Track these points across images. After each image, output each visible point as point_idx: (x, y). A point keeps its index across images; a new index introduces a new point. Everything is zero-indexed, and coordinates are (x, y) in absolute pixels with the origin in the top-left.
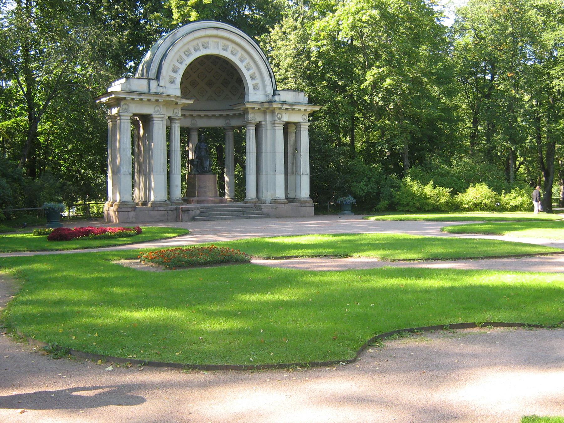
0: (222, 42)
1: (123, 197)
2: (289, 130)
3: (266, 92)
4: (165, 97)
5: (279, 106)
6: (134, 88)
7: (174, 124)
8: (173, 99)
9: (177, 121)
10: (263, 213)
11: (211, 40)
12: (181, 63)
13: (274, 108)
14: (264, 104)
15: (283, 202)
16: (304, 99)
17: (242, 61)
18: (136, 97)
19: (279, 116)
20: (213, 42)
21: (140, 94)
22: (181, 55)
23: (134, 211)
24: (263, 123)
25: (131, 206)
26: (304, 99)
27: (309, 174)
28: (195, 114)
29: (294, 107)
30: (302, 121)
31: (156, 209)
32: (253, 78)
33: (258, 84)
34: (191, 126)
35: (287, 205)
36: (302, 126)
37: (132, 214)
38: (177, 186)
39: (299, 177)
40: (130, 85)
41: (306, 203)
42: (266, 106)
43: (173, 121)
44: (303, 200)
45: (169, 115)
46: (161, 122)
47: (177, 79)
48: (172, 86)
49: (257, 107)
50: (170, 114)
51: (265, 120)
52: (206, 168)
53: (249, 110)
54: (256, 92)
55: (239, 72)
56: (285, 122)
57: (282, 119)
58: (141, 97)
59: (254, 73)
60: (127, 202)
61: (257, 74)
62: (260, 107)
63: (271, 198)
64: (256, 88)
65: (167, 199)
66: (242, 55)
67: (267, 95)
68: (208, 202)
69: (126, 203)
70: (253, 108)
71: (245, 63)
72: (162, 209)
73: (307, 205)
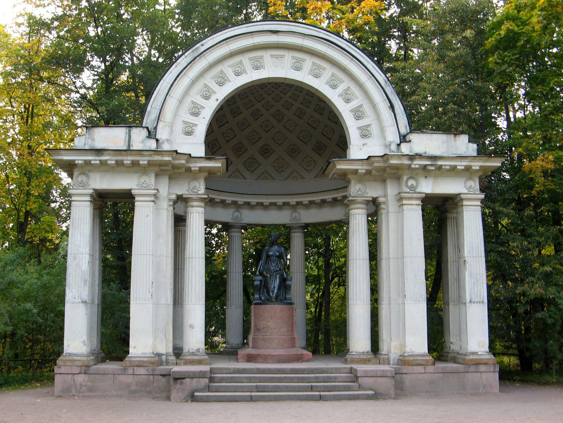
0: (289, 57)
1: (68, 346)
2: (449, 215)
3: (385, 140)
4: (150, 155)
5: (406, 162)
6: (99, 145)
7: (190, 210)
8: (167, 158)
9: (195, 204)
10: (360, 388)
11: (267, 55)
12: (207, 98)
13: (397, 168)
14: (373, 159)
15: (424, 363)
16: (467, 148)
17: (334, 87)
18: (94, 159)
19: (411, 182)
20: (272, 56)
21: (99, 152)
22: (208, 84)
23: (85, 373)
24: (381, 200)
25: (81, 364)
26: (467, 148)
27: (486, 301)
28: (293, 200)
29: (440, 163)
30: (466, 191)
31: (130, 371)
32: (358, 114)
33: (369, 126)
34: (290, 222)
35: (431, 369)
36: (465, 203)
37: (81, 379)
38: (192, 326)
39: (462, 306)
40: (93, 140)
41: (478, 363)
42: (379, 164)
43: (189, 204)
44: (471, 357)
45: (180, 193)
46: (152, 203)
47: (199, 127)
48: (190, 139)
49: (362, 168)
50: (182, 189)
51: (385, 196)
52: (273, 291)
53: (350, 176)
54: (365, 141)
55: (330, 105)
56: (424, 195)
57: (418, 190)
58: (104, 158)
59: (361, 106)
60: (76, 355)
61: (367, 108)
62: (369, 168)
63: (399, 352)
64: (365, 133)
65: (171, 350)
66: (333, 75)
67: (388, 146)
68: (265, 359)
69: (71, 358)
70: (356, 172)
71: (341, 88)
72: (142, 371)
73: (482, 368)
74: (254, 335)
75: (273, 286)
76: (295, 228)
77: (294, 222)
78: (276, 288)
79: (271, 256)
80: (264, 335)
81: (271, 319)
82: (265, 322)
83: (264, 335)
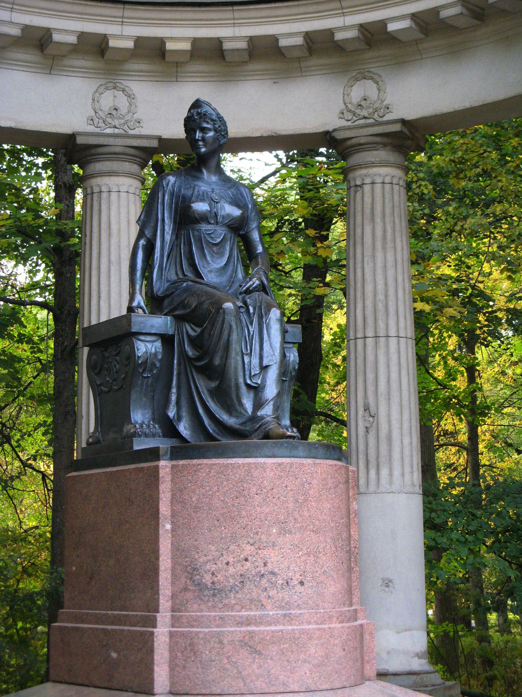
34: (91, 129)
74: (175, 621)
75: (255, 361)
76: (115, 156)
77: (109, 131)
78: (273, 374)
79: (204, 218)
80: (248, 622)
81: (283, 532)
82: (248, 549)
83: (248, 622)
